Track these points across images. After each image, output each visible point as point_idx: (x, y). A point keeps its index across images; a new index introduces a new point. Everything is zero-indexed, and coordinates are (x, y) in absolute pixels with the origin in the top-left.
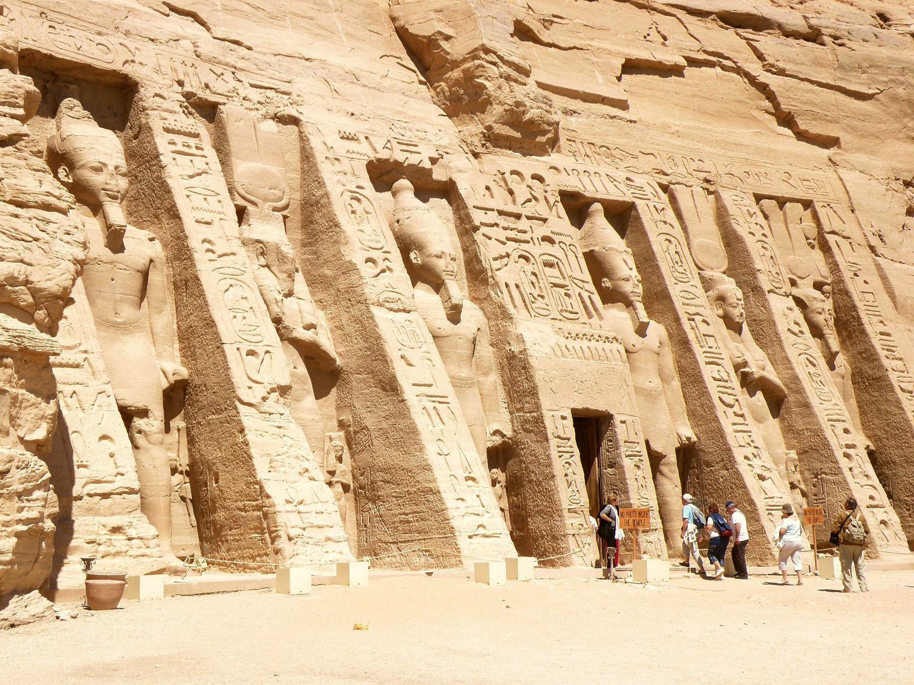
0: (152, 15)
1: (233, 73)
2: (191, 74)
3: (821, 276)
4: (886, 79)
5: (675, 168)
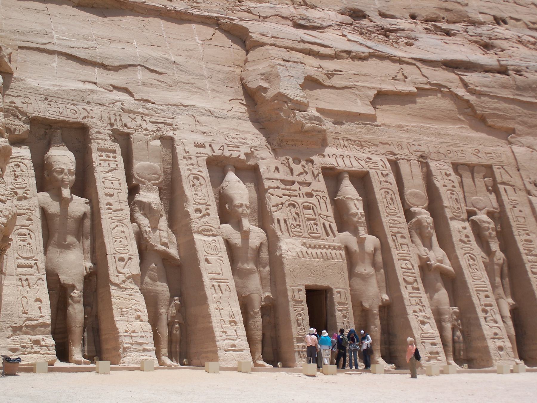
0: (103, 92)
1: (142, 117)
2: (118, 120)
3: (493, 208)
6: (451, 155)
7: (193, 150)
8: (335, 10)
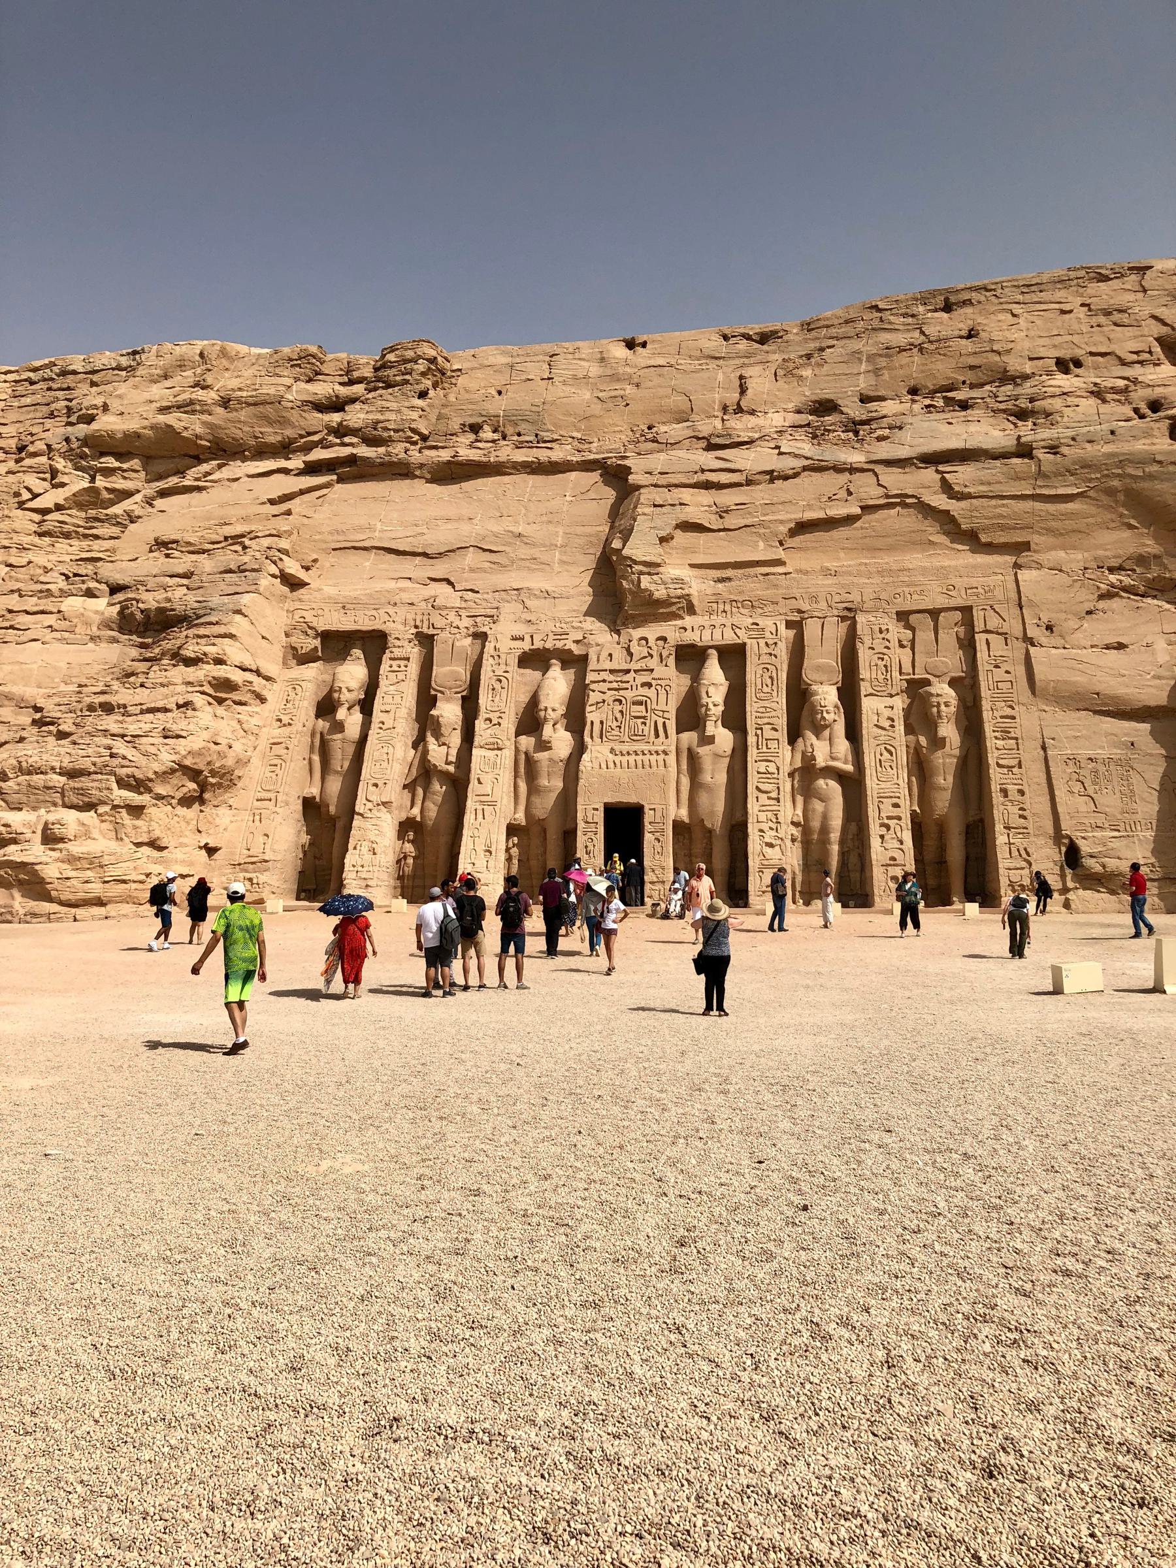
4: (1098, 476)
6: (899, 600)
7: (505, 644)
8: (785, 410)
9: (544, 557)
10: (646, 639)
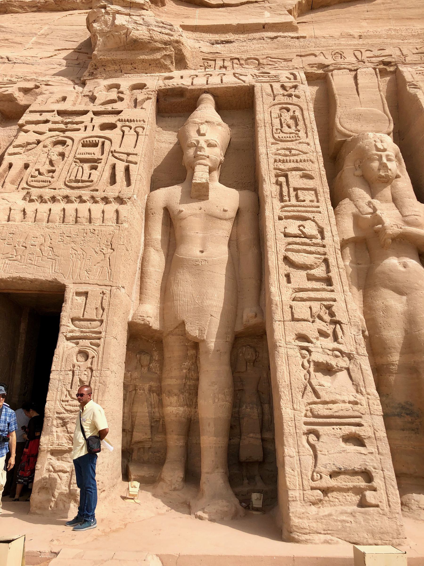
5: (339, 60)
9: (18, 39)
10: (117, 86)
